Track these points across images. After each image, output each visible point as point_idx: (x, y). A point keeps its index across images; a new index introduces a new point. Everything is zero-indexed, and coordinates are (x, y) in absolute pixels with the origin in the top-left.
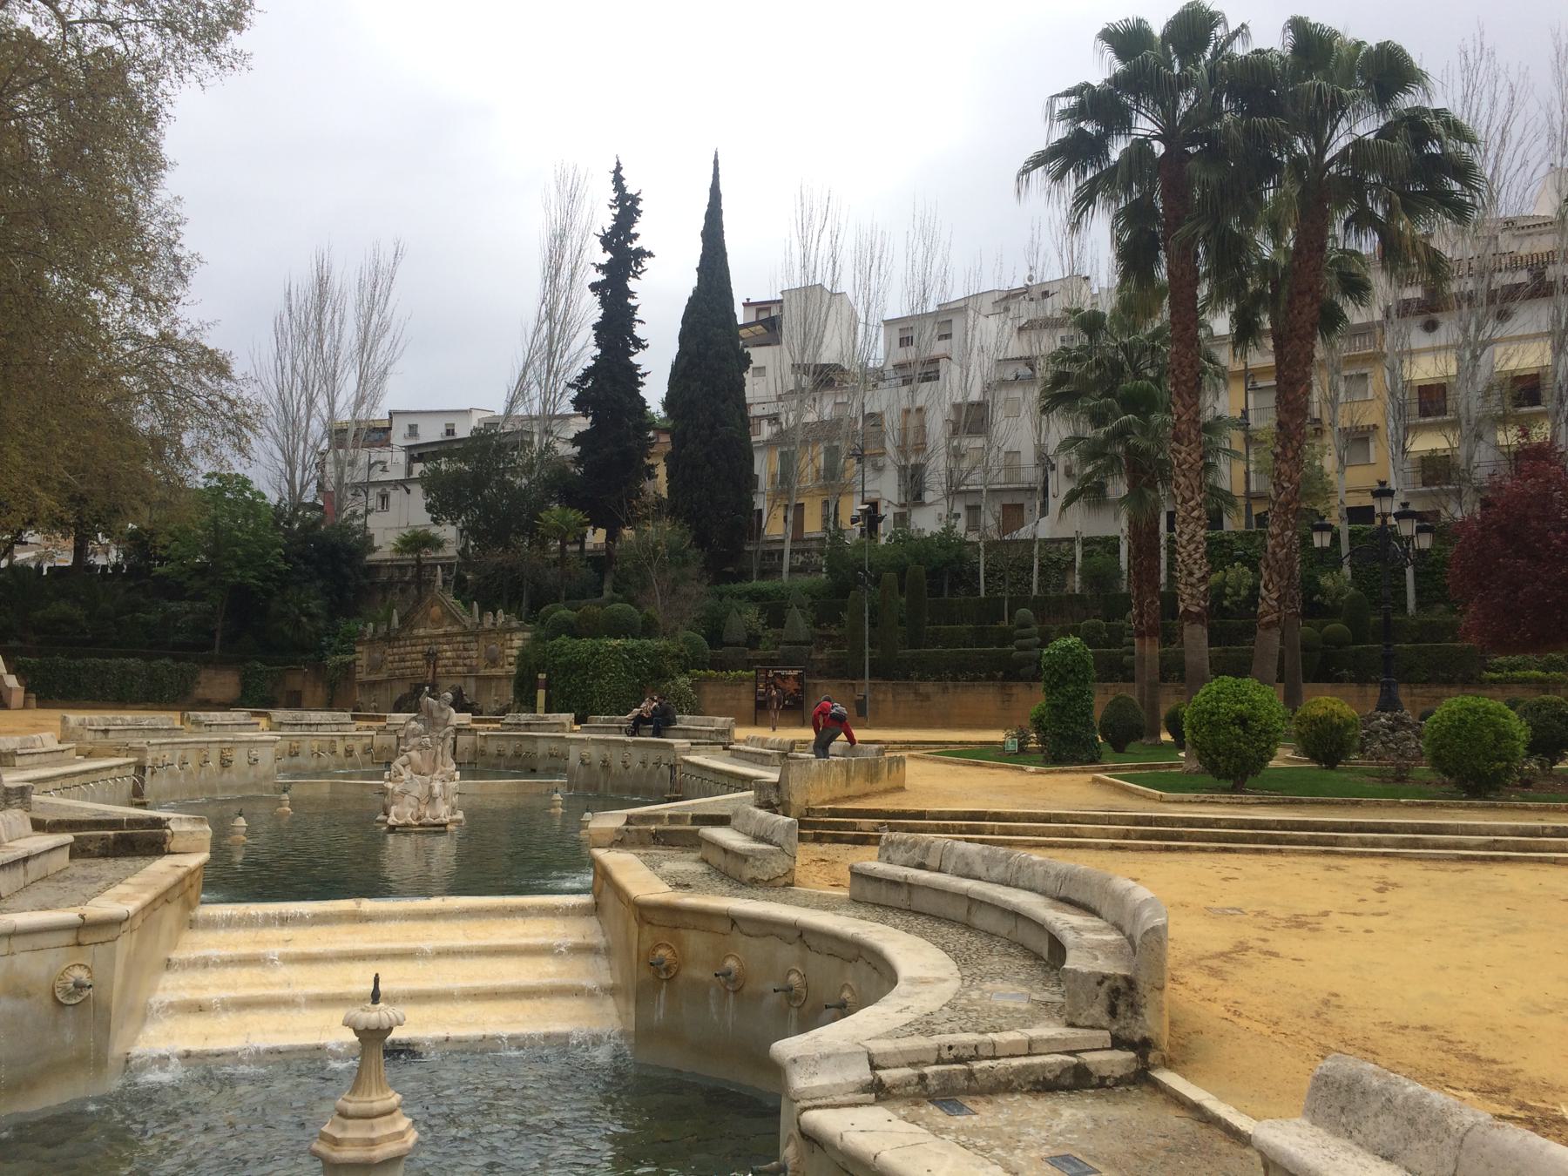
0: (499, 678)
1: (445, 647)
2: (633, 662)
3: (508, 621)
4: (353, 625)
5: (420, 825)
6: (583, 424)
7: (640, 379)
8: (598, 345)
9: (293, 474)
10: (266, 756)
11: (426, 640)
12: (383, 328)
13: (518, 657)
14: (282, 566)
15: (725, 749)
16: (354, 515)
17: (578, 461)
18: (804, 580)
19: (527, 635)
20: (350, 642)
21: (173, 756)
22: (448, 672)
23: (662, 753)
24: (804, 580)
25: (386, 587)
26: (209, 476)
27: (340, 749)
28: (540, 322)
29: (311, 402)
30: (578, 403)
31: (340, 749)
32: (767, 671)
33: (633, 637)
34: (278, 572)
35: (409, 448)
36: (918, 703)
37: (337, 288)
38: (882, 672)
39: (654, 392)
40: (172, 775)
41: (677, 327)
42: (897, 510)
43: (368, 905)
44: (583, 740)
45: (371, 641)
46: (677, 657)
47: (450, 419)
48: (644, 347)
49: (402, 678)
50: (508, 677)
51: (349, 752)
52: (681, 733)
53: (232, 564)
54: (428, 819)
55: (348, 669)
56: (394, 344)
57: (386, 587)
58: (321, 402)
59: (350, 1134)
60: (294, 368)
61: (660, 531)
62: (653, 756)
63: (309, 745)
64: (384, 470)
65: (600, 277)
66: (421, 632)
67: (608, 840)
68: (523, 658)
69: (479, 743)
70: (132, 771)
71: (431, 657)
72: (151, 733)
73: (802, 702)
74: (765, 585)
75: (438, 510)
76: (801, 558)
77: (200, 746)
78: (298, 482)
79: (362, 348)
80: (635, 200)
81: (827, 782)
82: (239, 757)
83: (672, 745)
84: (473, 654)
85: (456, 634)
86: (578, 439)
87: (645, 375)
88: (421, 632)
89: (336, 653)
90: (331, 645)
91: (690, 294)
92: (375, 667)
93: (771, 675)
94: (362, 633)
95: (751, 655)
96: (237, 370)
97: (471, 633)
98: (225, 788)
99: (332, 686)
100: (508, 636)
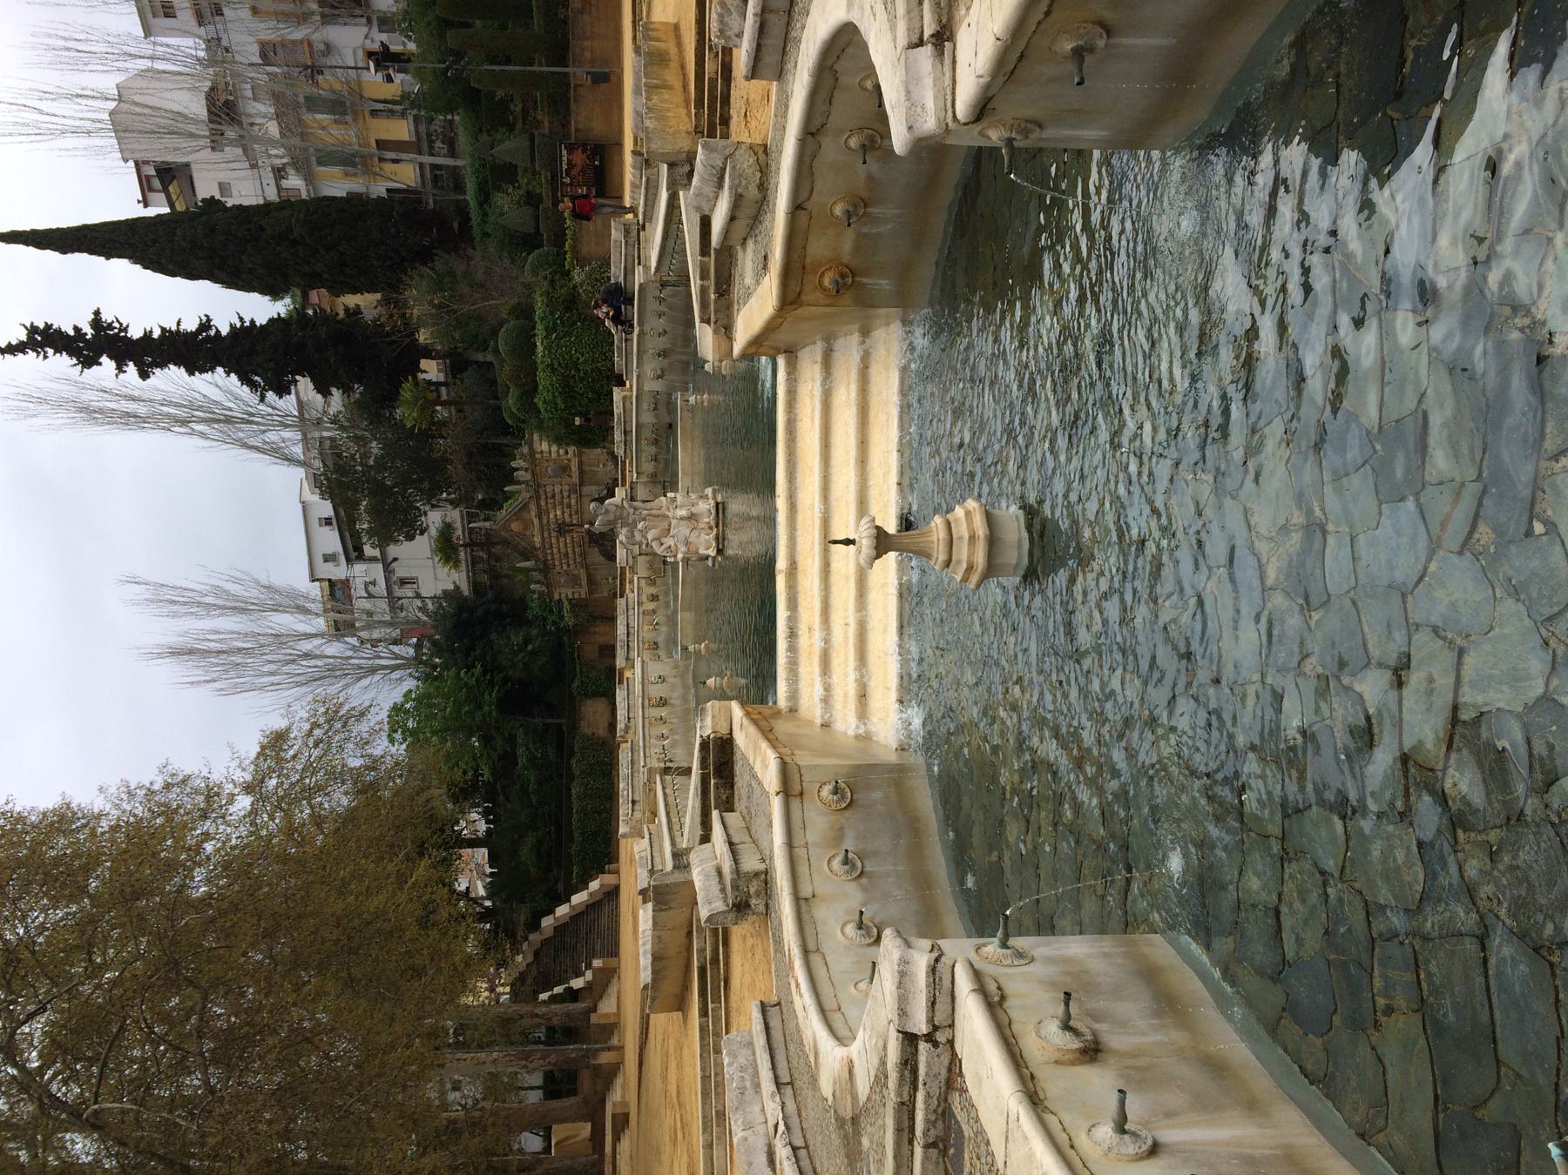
0: (581, 463)
1: (551, 516)
2: (559, 328)
3: (523, 456)
4: (534, 604)
5: (717, 526)
6: (305, 385)
7: (247, 324)
8: (212, 369)
9: (385, 667)
10: (655, 669)
11: (546, 534)
12: (218, 591)
13: (559, 445)
14: (478, 670)
15: (644, 229)
16: (423, 609)
17: (347, 390)
18: (463, 140)
19: (536, 437)
20: (550, 606)
21: (655, 746)
22: (577, 513)
23: (650, 297)
24: (463, 140)
25: (495, 575)
26: (392, 741)
27: (651, 606)
28: (192, 433)
29: (307, 656)
30: (282, 391)
31: (651, 606)
32: (563, 183)
33: (534, 328)
34: (484, 673)
35: (348, 560)
36: (594, 10)
37: (181, 639)
38: (560, 52)
39: (260, 308)
40: (673, 745)
41: (179, 282)
42: (375, 28)
43: (781, 564)
44: (638, 376)
45: (548, 586)
46: (552, 282)
47: (315, 523)
48: (209, 320)
49: (584, 555)
50: (580, 454)
51: (654, 598)
52: (629, 277)
53: (479, 713)
54: (711, 519)
55: (576, 605)
56: (237, 581)
57: (495, 575)
58: (306, 646)
59: (964, 557)
60: (272, 674)
61: (419, 301)
62: (652, 305)
63: (647, 633)
64: (374, 583)
65: (131, 368)
66: (537, 540)
67: (724, 343)
68: (559, 440)
69: (644, 479)
70: (668, 778)
71: (563, 529)
72: (636, 766)
73: (596, 146)
74: (471, 186)
75: (412, 529)
76: (438, 144)
77: (647, 724)
78: (393, 662)
79: (243, 611)
80: (33, 330)
81: (668, 110)
82: (656, 691)
83: (641, 285)
84: (557, 489)
85: (539, 506)
86: (323, 390)
87: (241, 319)
88: (537, 540)
89: (562, 617)
90: (554, 623)
91: (138, 267)
92: (575, 581)
93: (568, 180)
94: (541, 594)
95: (547, 203)
96: (280, 724)
97: (537, 492)
98: (685, 700)
99: (593, 618)
100: (538, 456)
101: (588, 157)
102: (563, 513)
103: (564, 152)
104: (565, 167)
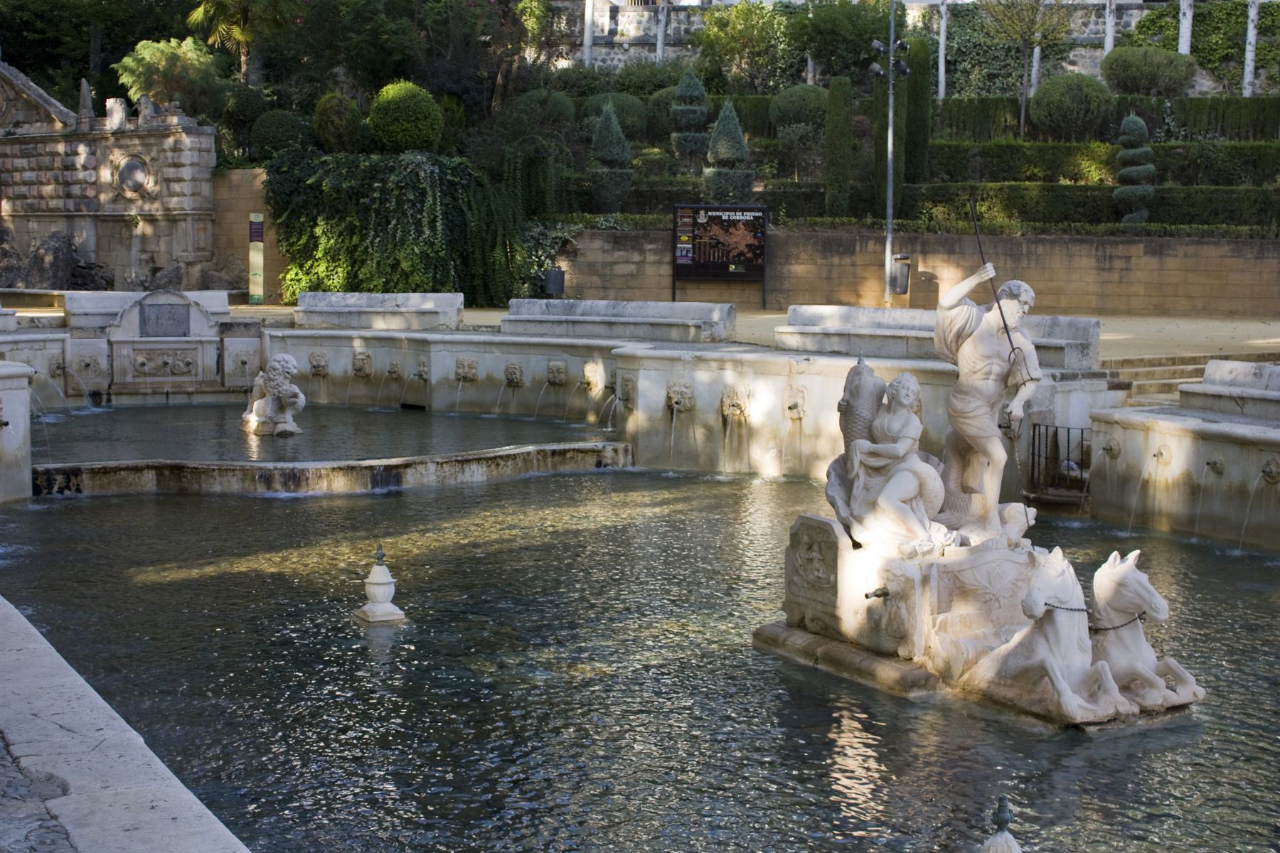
32: (696, 212)
93: (702, 219)
101: (742, 254)
103: (749, 216)
104: (725, 216)
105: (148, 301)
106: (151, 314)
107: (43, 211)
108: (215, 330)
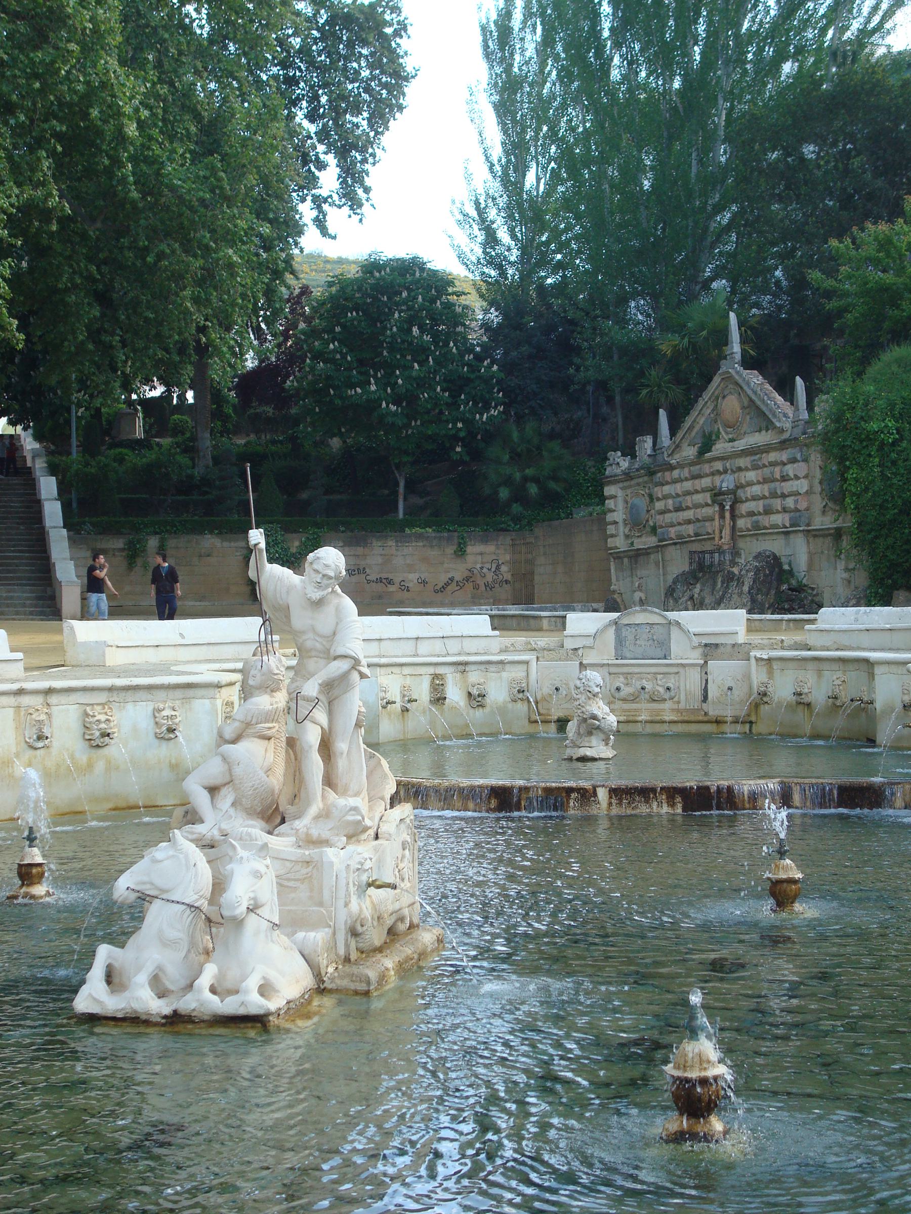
22: (757, 526)
51: (476, 699)
102: (754, 498)
105: (625, 621)
106: (627, 633)
107: (765, 528)
108: (698, 653)
